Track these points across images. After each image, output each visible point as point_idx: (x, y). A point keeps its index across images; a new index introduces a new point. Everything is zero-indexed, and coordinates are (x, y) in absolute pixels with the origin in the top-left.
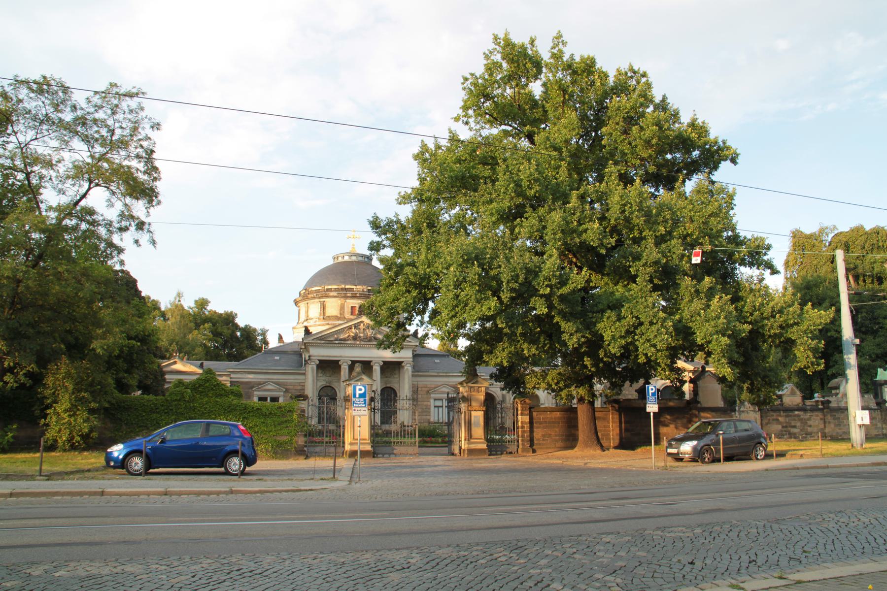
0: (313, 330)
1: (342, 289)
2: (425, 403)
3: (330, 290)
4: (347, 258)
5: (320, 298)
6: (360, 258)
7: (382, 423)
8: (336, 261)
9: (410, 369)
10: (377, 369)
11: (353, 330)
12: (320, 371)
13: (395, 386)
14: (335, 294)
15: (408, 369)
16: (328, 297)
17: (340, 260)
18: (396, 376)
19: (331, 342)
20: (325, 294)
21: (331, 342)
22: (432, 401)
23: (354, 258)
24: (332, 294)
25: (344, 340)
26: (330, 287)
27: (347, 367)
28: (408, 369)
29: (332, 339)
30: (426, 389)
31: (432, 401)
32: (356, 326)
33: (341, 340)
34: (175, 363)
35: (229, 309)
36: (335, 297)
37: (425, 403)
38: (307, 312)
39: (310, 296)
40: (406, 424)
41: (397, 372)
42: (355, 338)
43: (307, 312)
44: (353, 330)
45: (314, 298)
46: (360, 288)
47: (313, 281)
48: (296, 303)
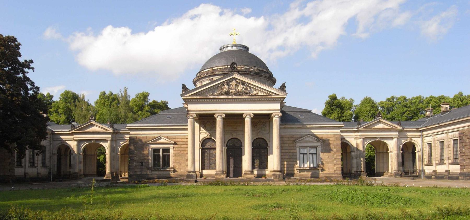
2: (292, 151)
4: (229, 49)
6: (240, 48)
8: (222, 51)
10: (248, 121)
11: (226, 86)
17: (225, 50)
18: (267, 128)
20: (213, 74)
22: (298, 149)
23: (234, 48)
30: (292, 139)
31: (298, 149)
32: (228, 83)
34: (92, 125)
35: (164, 100)
37: (292, 151)
42: (227, 93)
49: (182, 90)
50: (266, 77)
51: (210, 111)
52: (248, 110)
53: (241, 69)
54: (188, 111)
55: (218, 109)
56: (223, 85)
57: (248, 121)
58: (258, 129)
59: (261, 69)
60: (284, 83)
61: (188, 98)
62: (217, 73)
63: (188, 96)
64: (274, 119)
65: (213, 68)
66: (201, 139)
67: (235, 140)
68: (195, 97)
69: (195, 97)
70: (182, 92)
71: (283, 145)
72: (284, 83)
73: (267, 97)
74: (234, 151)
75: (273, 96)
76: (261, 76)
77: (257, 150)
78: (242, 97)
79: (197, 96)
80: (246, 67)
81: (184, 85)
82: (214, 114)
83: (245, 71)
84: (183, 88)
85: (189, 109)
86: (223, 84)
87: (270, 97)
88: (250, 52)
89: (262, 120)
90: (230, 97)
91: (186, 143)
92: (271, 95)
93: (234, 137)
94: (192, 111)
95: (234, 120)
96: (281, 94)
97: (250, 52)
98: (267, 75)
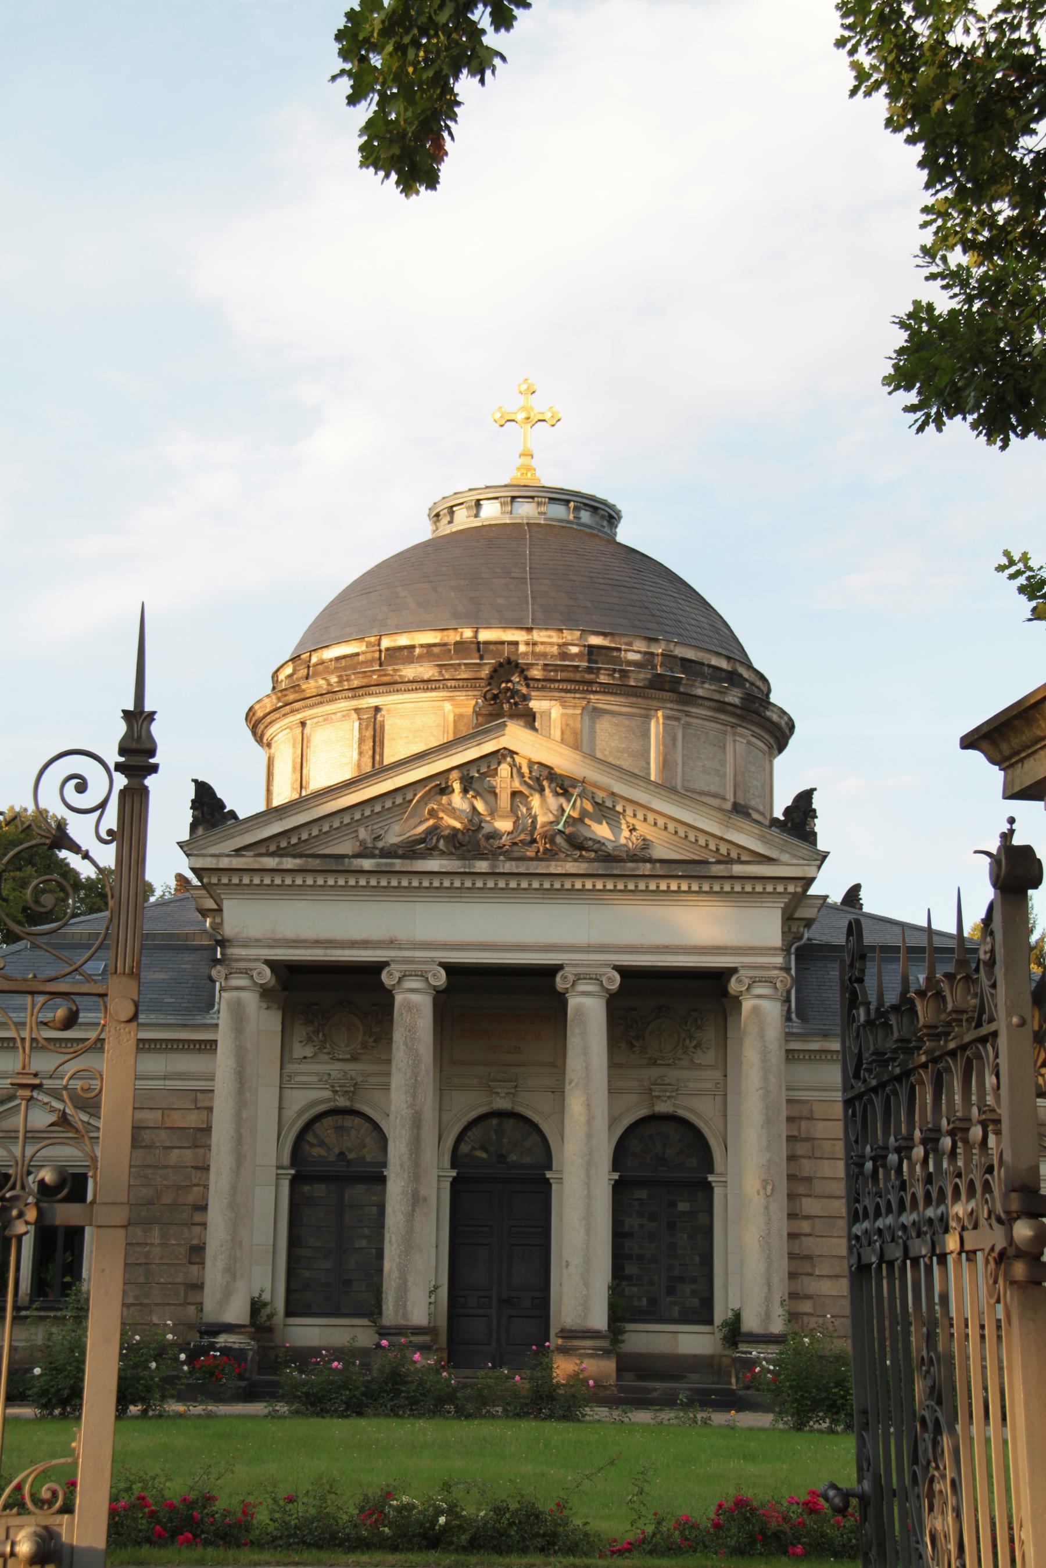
0: (242, 799)
1: (461, 646)
3: (405, 654)
4: (491, 512)
5: (356, 692)
6: (558, 511)
7: (620, 1313)
9: (773, 1010)
10: (588, 1010)
11: (457, 800)
12: (300, 1031)
13: (700, 1111)
14: (426, 670)
15: (762, 1011)
16: (392, 685)
18: (708, 1057)
19: (336, 865)
20: (381, 673)
21: (336, 865)
23: (526, 511)
24: (410, 672)
25: (412, 849)
26: (403, 640)
27: (424, 1003)
28: (762, 1011)
29: (346, 847)
32: (475, 777)
33: (389, 853)
36: (425, 684)
38: (301, 766)
39: (310, 687)
40: (751, 1323)
41: (709, 1035)
43: (301, 766)
44: (457, 800)
45: (329, 695)
46: (547, 639)
47: (327, 626)
48: (257, 725)
49: (188, 816)
50: (722, 707)
51: (353, 944)
52: (589, 949)
53: (564, 656)
54: (223, 943)
55: (402, 934)
56: (445, 790)
57: (588, 1010)
58: (653, 1063)
59: (690, 654)
60: (813, 790)
61: (225, 863)
62: (410, 672)
63: (222, 851)
64: (747, 1005)
65: (386, 643)
66: (290, 1113)
67: (509, 1124)
68: (271, 862)
69: (271, 862)
70: (193, 827)
71: (807, 1167)
72: (815, 789)
73: (702, 870)
74: (499, 1191)
75: (738, 869)
76: (689, 699)
77: (643, 1194)
78: (554, 868)
79: (279, 853)
80: (595, 640)
81: (195, 781)
82: (377, 968)
83: (589, 670)
84: (196, 805)
85: (229, 929)
86: (439, 785)
87: (718, 870)
88: (625, 534)
89: (671, 1007)
90: (482, 866)
91: (201, 1136)
92: (728, 861)
93: (502, 1104)
94: (247, 944)
95: (500, 1006)
96: (785, 857)
97: (625, 534)
98: (734, 697)
